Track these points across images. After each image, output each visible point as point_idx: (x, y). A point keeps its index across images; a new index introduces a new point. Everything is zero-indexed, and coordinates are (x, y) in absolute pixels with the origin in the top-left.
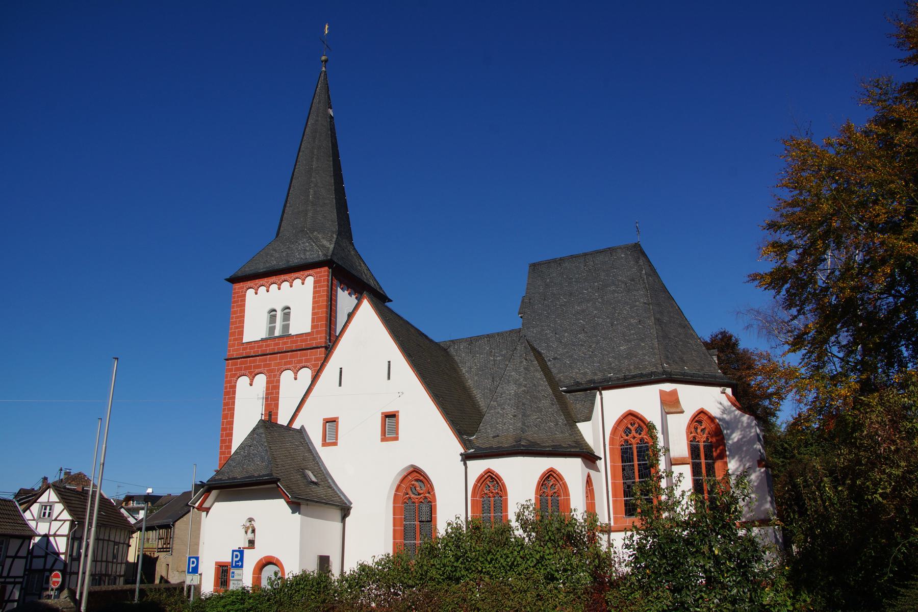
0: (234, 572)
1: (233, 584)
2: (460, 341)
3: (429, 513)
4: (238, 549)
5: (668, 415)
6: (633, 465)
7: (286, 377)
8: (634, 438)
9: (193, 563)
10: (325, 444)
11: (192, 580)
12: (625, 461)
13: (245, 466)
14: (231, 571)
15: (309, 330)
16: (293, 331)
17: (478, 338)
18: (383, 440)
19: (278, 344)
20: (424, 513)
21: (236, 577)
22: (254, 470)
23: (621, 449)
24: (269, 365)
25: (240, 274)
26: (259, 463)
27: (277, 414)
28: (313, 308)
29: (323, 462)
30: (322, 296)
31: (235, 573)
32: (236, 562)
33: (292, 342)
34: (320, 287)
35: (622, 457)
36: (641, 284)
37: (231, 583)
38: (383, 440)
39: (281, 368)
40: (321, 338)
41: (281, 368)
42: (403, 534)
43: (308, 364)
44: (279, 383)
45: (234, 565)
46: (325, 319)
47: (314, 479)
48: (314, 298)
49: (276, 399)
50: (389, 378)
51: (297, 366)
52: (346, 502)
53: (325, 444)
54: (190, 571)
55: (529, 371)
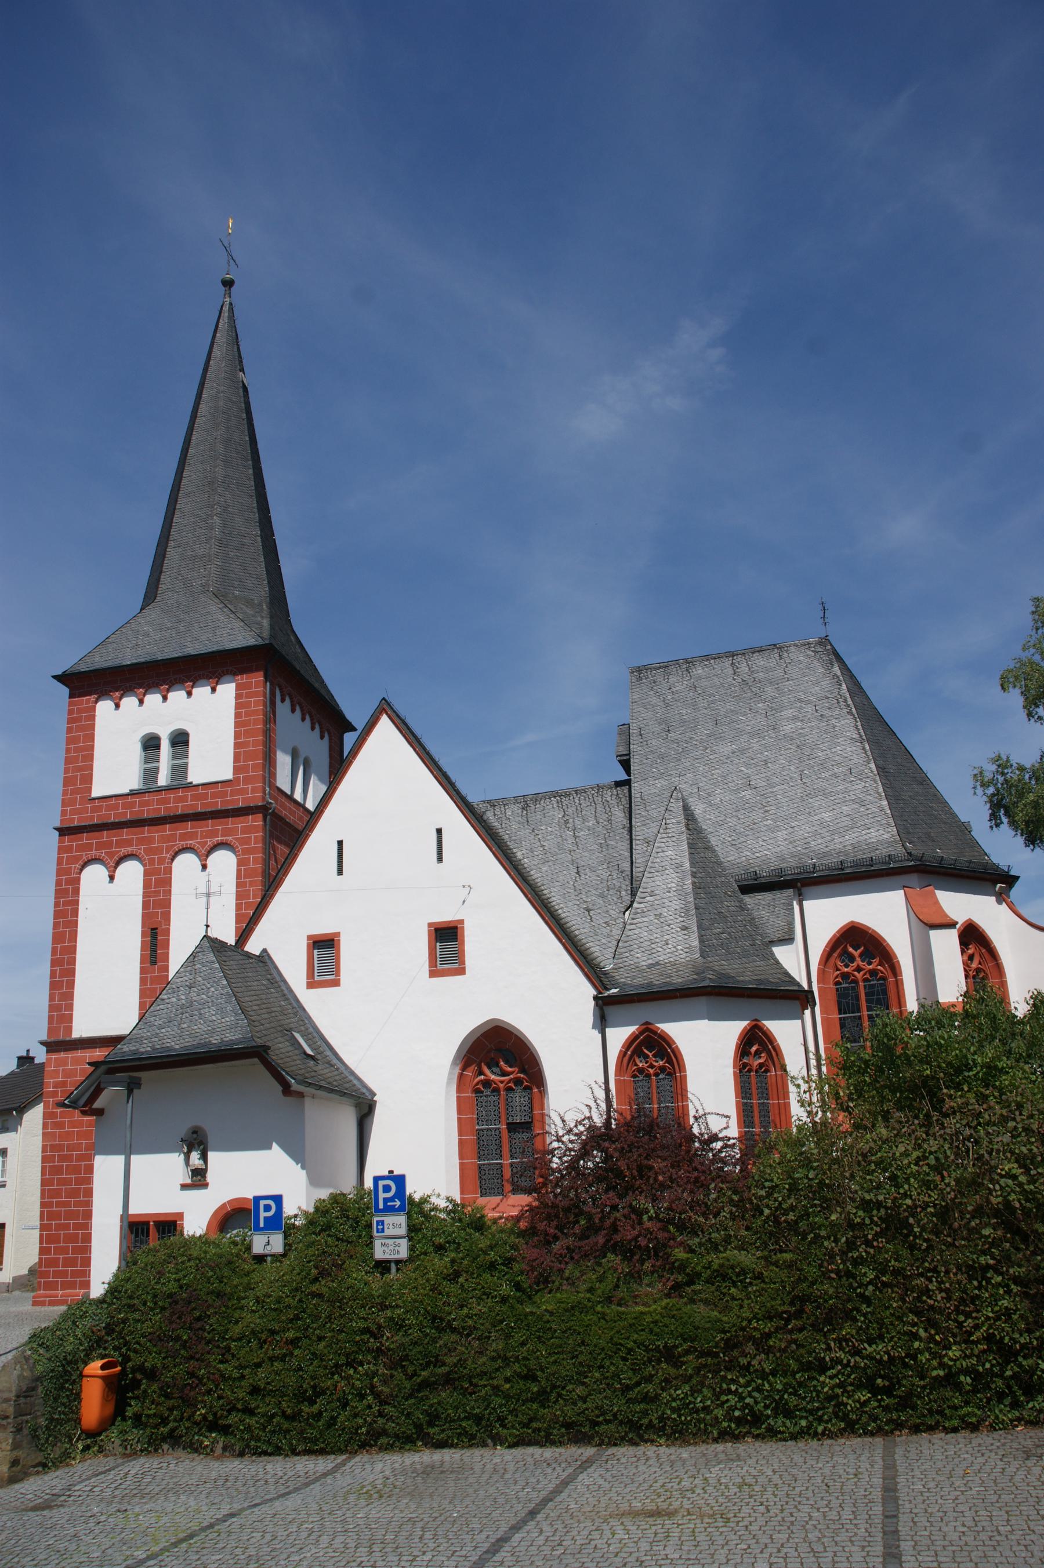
0: (383, 1222)
1: (383, 1245)
2: (504, 802)
3: (527, 1108)
4: (387, 1173)
5: (933, 934)
6: (860, 1018)
7: (185, 866)
8: (859, 969)
9: (267, 1208)
10: (312, 984)
11: (268, 1243)
12: (845, 1009)
13: (185, 1026)
14: (375, 1219)
15: (228, 774)
16: (196, 776)
17: (537, 798)
18: (433, 974)
19: (167, 801)
20: (518, 1108)
21: (387, 1232)
22: (207, 1032)
23: (837, 990)
24: (150, 840)
25: (101, 661)
26: (214, 1018)
27: (167, 932)
28: (237, 735)
29: (310, 1018)
30: (255, 713)
31: (386, 1223)
32: (385, 1200)
33: (194, 798)
34: (248, 696)
35: (839, 1003)
36: (843, 707)
37: (377, 1243)
38: (433, 974)
39: (175, 845)
40: (254, 790)
41: (175, 845)
42: (477, 1148)
43: (230, 838)
44: (171, 873)
45: (381, 1206)
46: (261, 755)
47: (309, 1052)
48: (237, 715)
49: (166, 904)
50: (440, 859)
51: (206, 843)
52: (364, 1091)
53: (312, 984)
54: (262, 1225)
55: (696, 849)
